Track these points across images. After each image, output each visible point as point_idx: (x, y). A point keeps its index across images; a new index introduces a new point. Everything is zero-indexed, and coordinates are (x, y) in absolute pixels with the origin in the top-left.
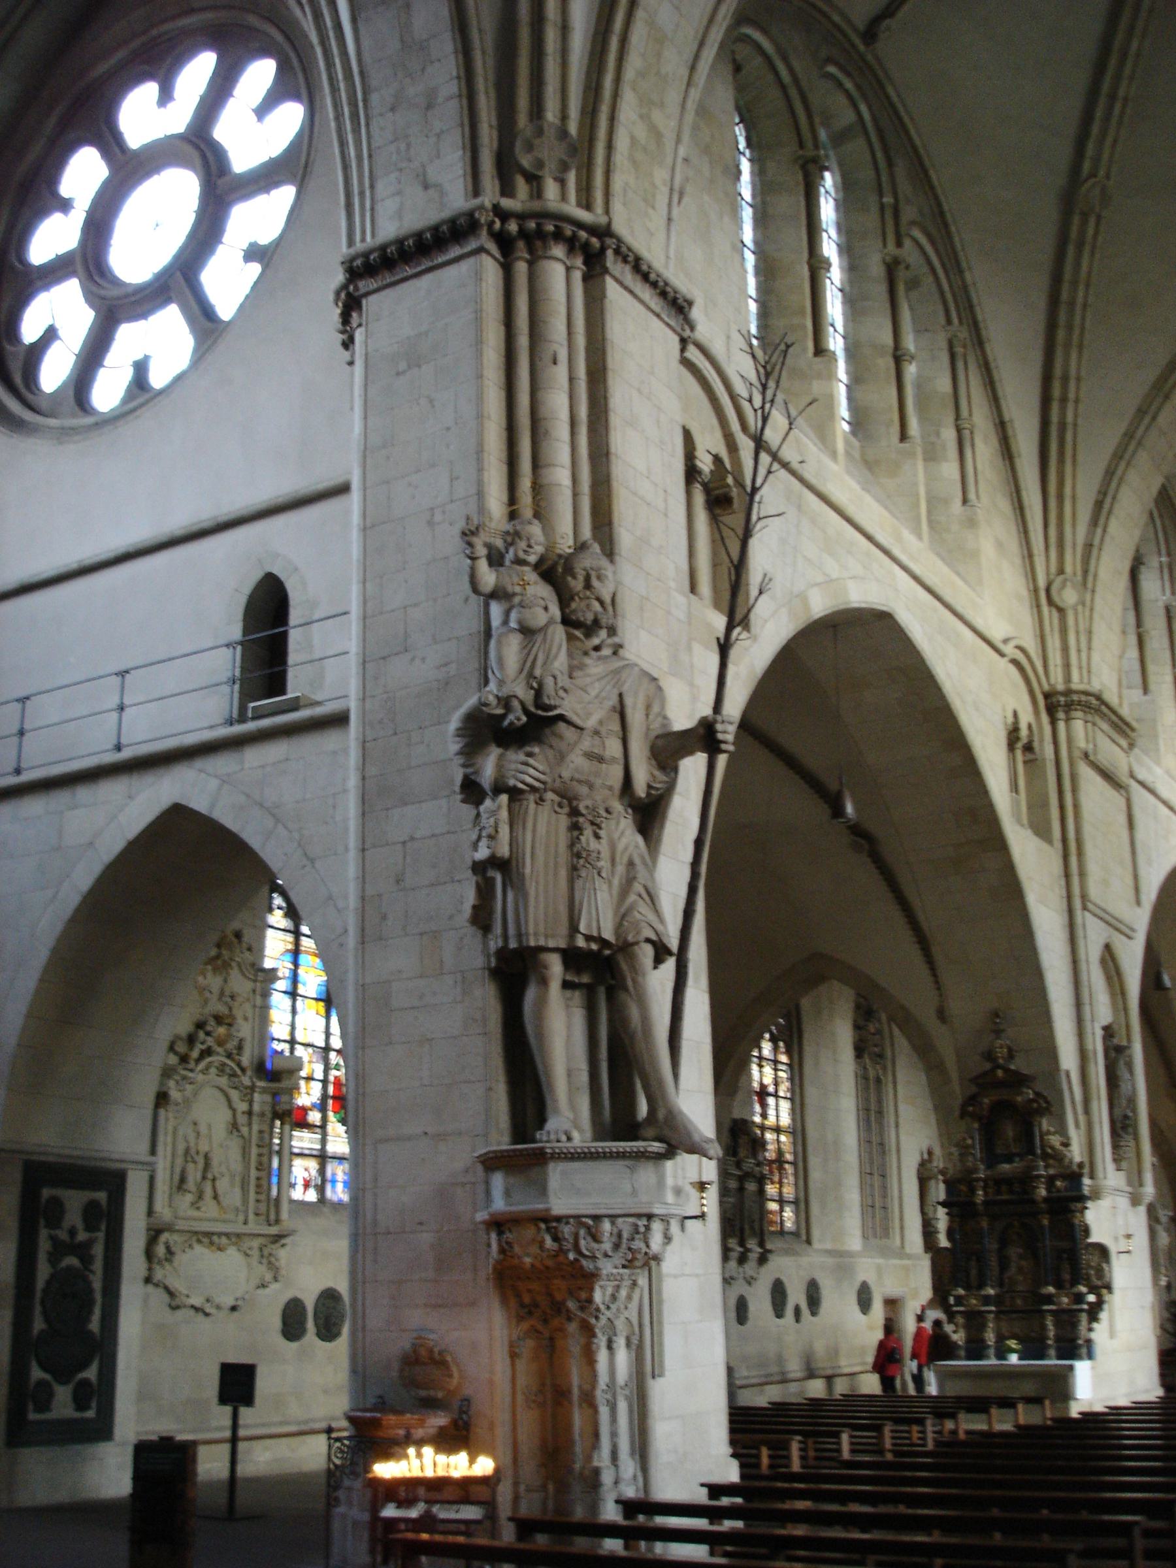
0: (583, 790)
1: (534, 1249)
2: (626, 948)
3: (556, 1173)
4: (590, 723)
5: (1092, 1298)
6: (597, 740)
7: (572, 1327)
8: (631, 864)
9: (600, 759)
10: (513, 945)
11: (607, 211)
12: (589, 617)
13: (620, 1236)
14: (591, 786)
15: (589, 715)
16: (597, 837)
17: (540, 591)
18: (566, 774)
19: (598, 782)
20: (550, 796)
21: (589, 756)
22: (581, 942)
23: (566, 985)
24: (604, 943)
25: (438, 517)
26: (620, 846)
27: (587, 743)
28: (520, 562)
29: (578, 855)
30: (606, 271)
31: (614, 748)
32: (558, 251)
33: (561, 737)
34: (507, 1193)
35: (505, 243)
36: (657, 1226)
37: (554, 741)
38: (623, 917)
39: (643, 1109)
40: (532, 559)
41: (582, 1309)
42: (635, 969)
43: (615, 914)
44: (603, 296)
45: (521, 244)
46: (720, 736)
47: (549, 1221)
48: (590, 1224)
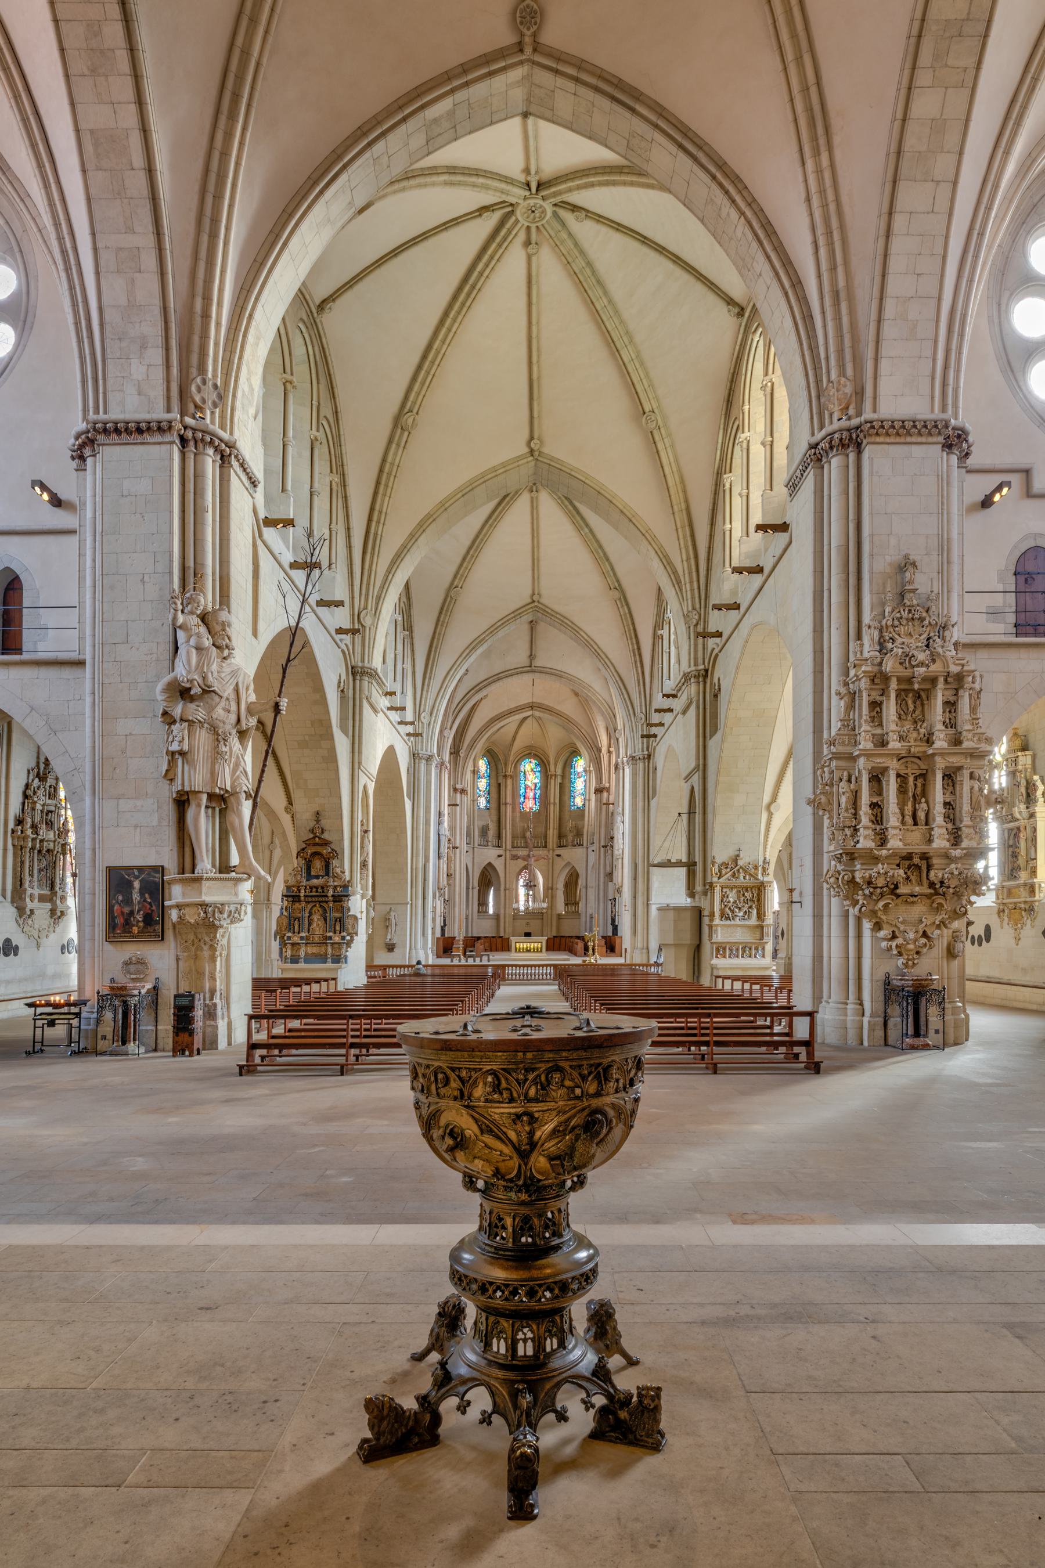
0: (221, 725)
1: (196, 917)
2: (235, 794)
3: (205, 884)
4: (225, 695)
5: (348, 938)
6: (227, 703)
7: (206, 948)
8: (238, 757)
9: (229, 711)
10: (187, 789)
11: (231, 433)
12: (224, 643)
13: (230, 912)
14: (224, 723)
15: (225, 691)
16: (226, 746)
17: (203, 629)
18: (214, 717)
19: (227, 721)
20: (206, 725)
21: (224, 709)
22: (217, 791)
23: (207, 807)
24: (227, 791)
25: (146, 578)
26: (234, 749)
27: (223, 703)
28: (192, 613)
29: (218, 753)
30: (232, 466)
31: (234, 707)
32: (210, 451)
33: (213, 700)
34: (184, 894)
35: (183, 441)
36: (243, 908)
37: (209, 701)
38: (235, 781)
39: (235, 860)
40: (199, 612)
41: (211, 940)
42: (239, 803)
43: (231, 778)
44: (229, 480)
45: (192, 443)
46: (281, 708)
47: (204, 905)
48: (220, 908)
